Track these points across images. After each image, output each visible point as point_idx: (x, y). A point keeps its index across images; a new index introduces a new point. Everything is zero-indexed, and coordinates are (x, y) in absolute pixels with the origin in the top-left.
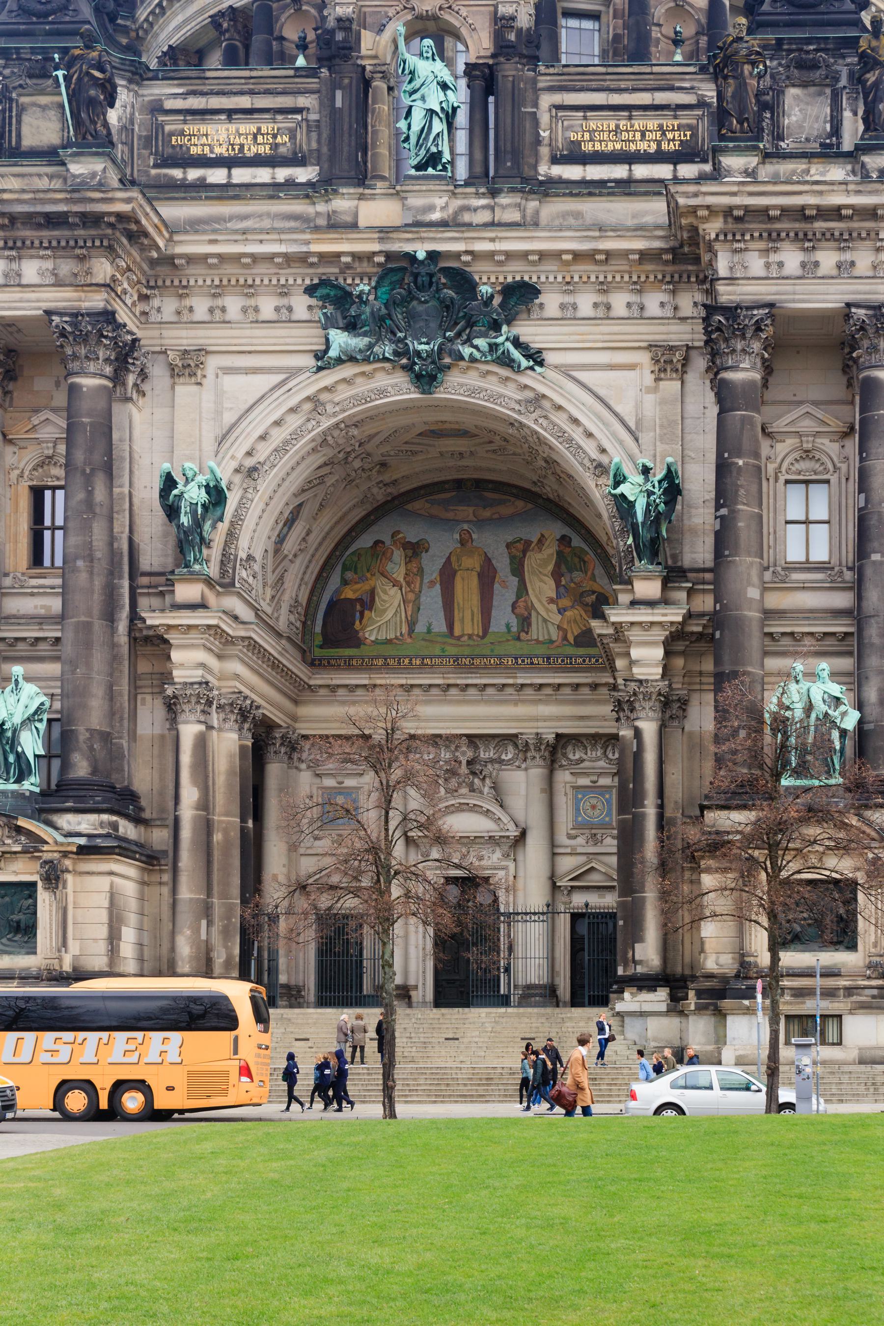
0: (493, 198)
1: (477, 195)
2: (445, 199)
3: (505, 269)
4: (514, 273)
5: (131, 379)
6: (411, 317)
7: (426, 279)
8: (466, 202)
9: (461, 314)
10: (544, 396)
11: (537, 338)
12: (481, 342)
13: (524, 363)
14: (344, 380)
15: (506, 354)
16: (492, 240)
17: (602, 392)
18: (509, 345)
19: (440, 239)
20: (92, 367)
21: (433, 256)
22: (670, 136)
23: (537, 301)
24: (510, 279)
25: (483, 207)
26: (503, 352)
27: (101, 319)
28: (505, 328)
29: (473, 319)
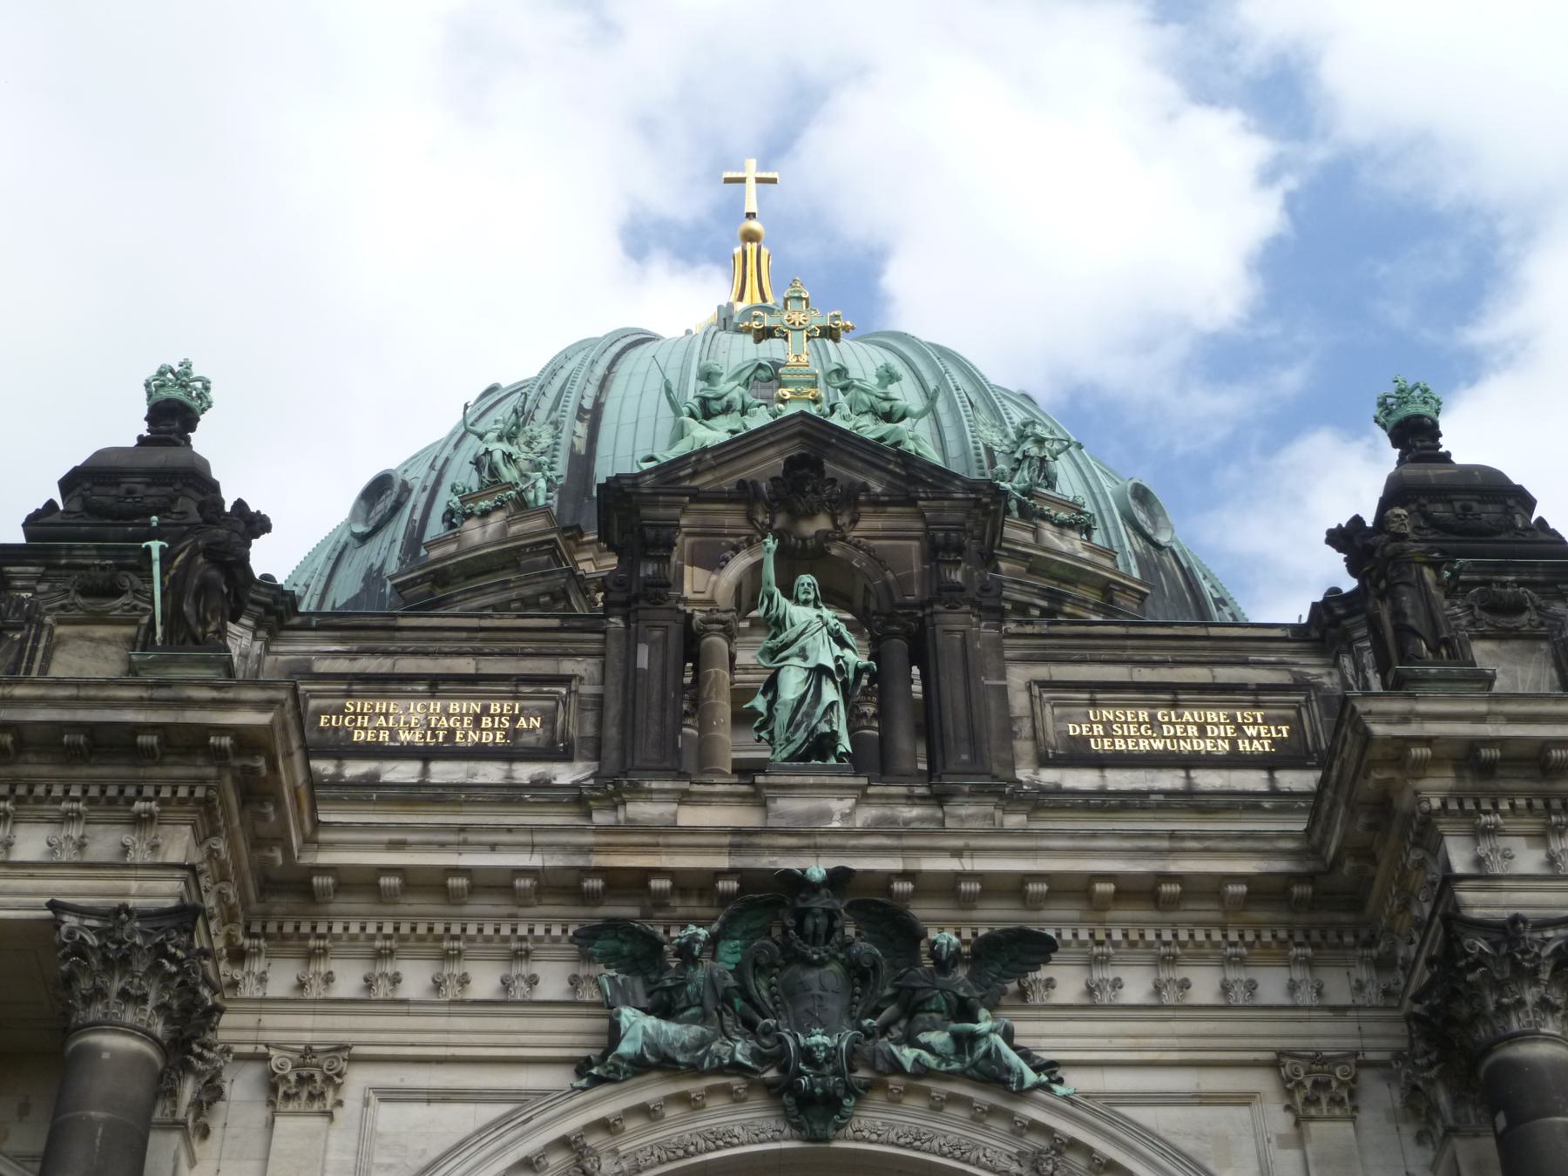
0: (941, 805)
1: (911, 799)
2: (849, 803)
3: (976, 914)
4: (997, 916)
5: (188, 1090)
6: (792, 994)
7: (822, 921)
8: (887, 811)
9: (888, 991)
10: (1074, 1144)
11: (1044, 1043)
12: (938, 1038)
13: (1031, 1077)
14: (644, 1111)
15: (992, 1056)
16: (957, 853)
17: (1188, 1145)
18: (997, 1039)
19: (854, 848)
20: (129, 1016)
21: (839, 879)
22: (1251, 731)
23: (1044, 973)
24: (982, 932)
25: (921, 819)
26: (987, 1054)
27: (167, 924)
28: (983, 1013)
29: (919, 996)
